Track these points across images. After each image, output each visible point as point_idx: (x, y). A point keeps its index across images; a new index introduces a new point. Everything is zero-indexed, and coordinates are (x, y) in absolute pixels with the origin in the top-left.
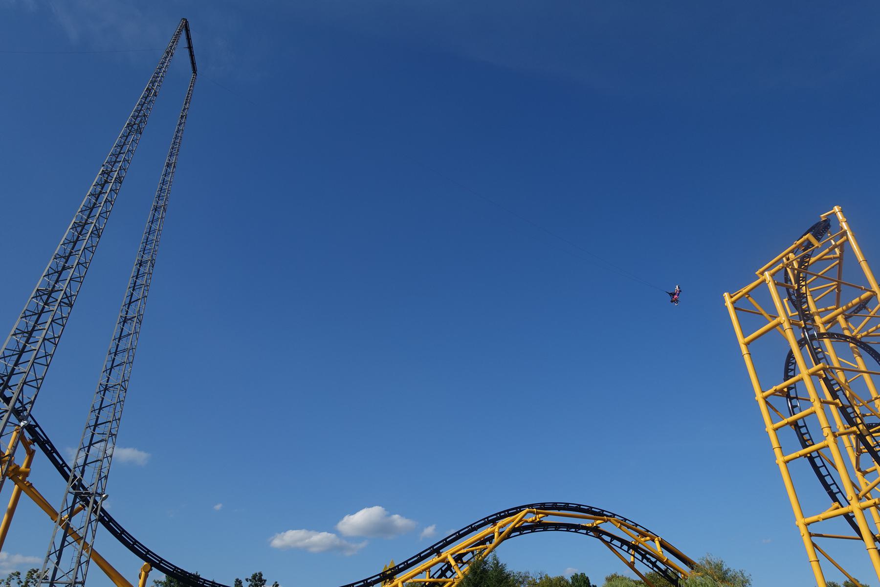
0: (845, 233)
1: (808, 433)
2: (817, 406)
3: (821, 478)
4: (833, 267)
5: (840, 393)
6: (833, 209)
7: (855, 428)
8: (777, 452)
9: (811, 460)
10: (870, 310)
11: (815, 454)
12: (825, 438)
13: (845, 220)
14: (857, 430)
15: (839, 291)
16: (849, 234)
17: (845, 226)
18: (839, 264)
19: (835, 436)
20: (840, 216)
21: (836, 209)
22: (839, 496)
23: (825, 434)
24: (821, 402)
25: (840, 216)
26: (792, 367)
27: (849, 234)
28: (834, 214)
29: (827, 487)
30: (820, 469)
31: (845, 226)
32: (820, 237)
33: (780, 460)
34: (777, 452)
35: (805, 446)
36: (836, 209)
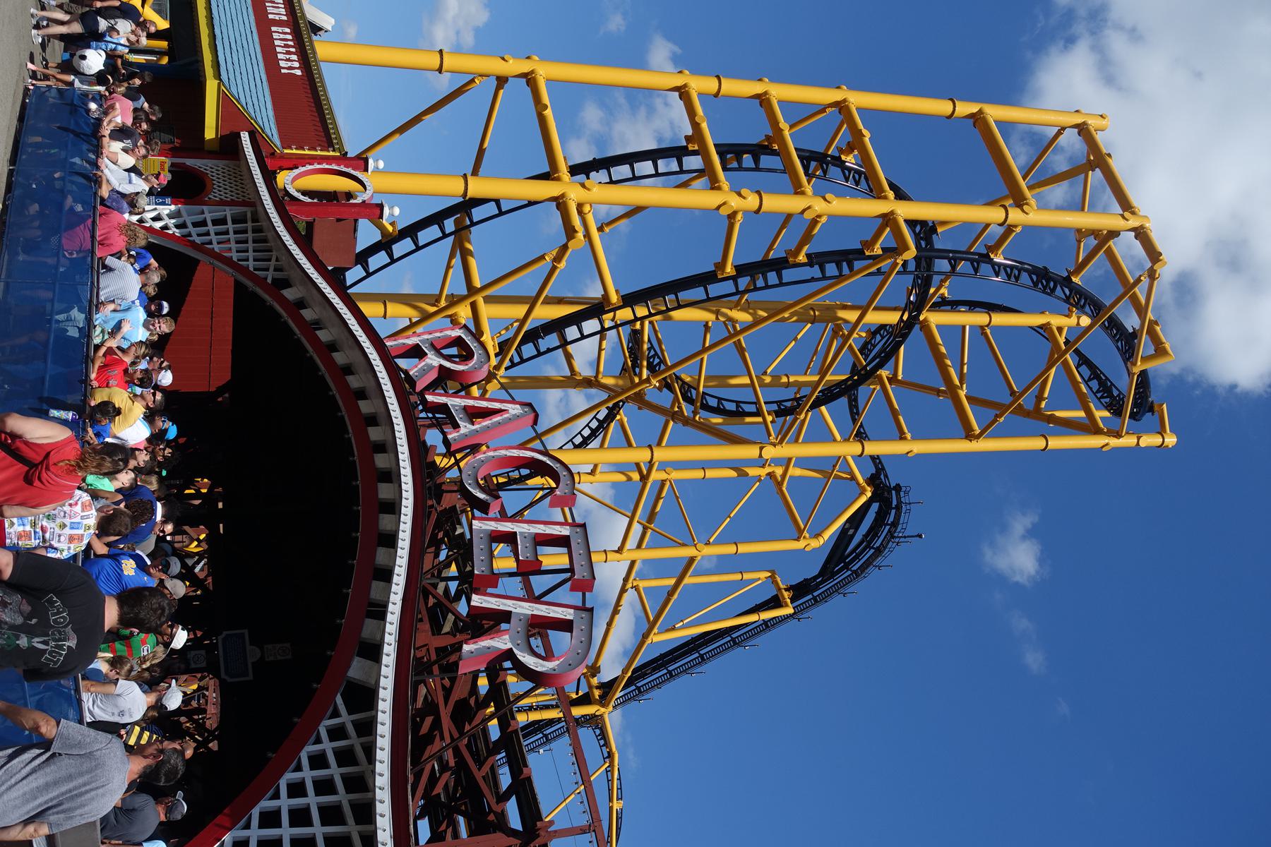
1: (740, 169)
5: (815, 272)
6: (1170, 431)
7: (729, 270)
8: (710, 85)
11: (693, 162)
14: (725, 275)
17: (1128, 441)
20: (1150, 440)
21: (1171, 440)
22: (602, 175)
25: (1150, 440)
28: (1161, 432)
31: (1128, 441)
34: (710, 85)
36: (1171, 440)
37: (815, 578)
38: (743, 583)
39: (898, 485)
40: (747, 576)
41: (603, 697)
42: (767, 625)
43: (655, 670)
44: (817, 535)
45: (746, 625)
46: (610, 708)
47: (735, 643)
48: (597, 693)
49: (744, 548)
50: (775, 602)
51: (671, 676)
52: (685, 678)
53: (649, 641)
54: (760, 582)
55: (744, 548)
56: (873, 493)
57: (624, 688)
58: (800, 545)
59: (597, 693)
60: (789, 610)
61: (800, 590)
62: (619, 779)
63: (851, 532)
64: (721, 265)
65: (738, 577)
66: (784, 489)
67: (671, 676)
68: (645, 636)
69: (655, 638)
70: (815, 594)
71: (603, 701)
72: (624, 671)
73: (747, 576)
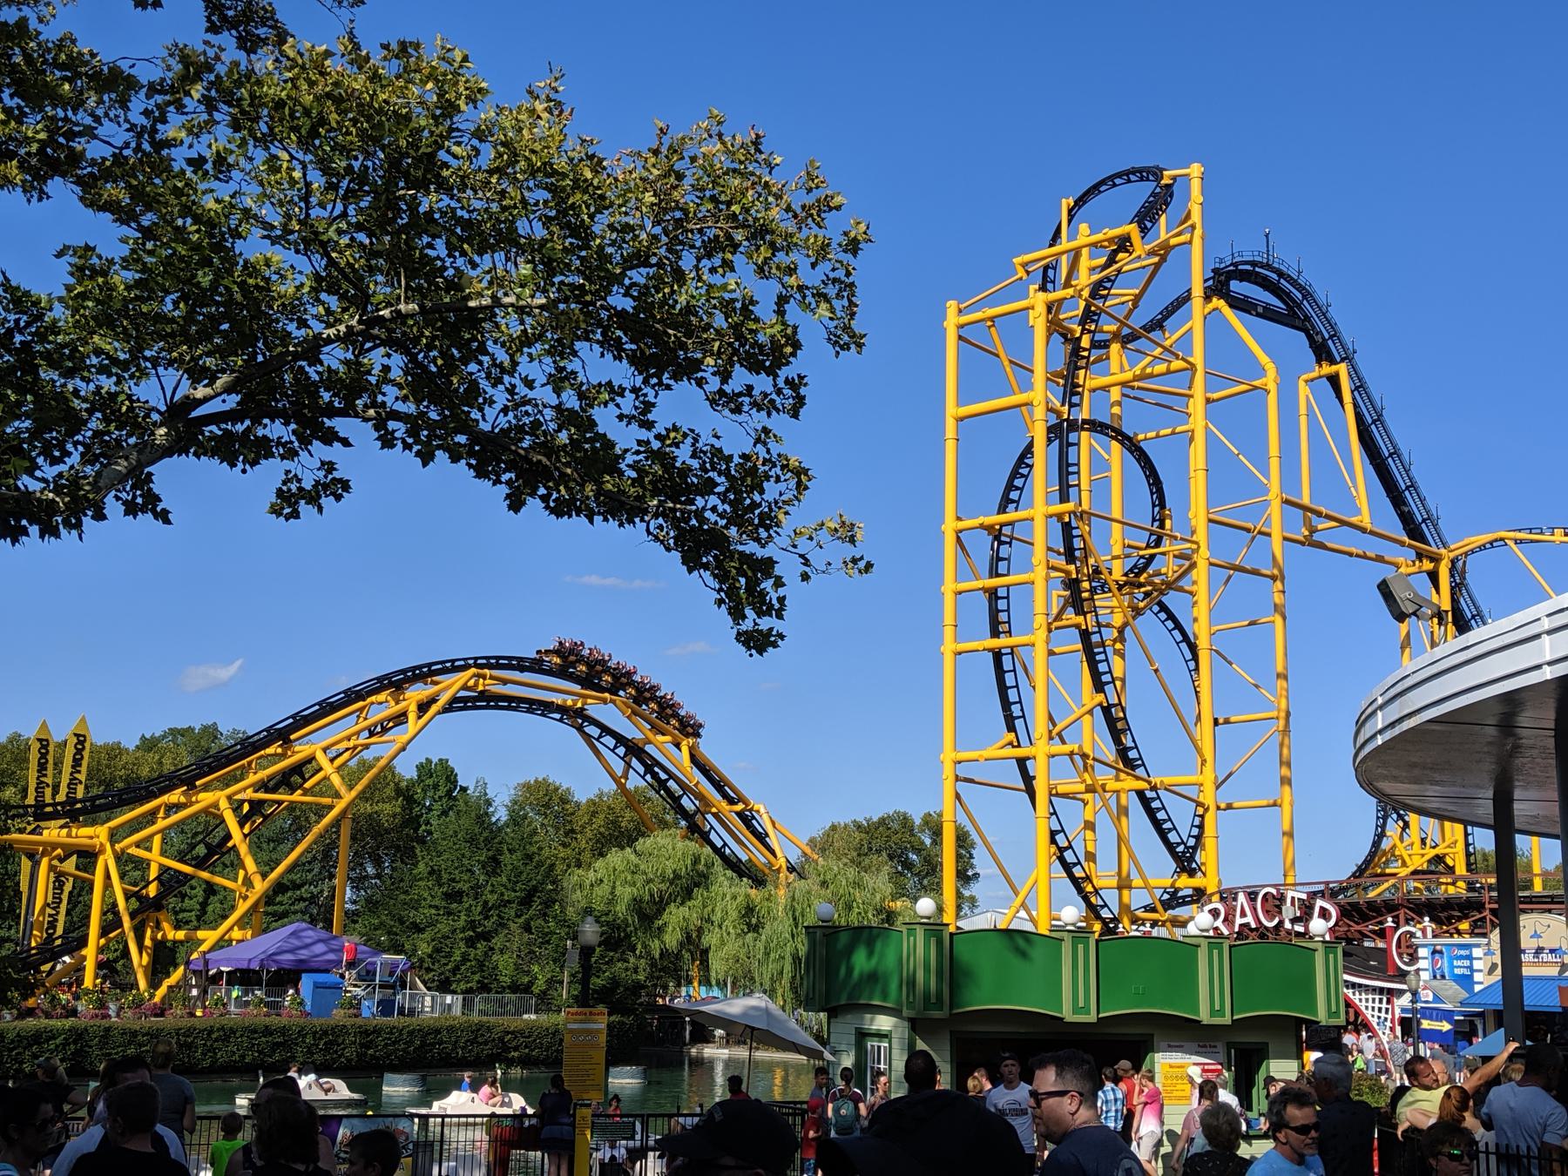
0: (1193, 227)
2: (1040, 573)
3: (1003, 689)
4: (1144, 267)
7: (1080, 619)
9: (997, 656)
10: (1167, 335)
12: (1031, 631)
13: (1201, 200)
15: (1135, 306)
16: (1198, 232)
18: (1157, 266)
19: (1050, 631)
20: (1196, 185)
21: (1195, 170)
23: (1036, 626)
24: (1048, 568)
25: (1196, 185)
26: (1024, 471)
27: (1198, 232)
29: (1006, 704)
30: (1007, 675)
32: (1149, 225)
33: (949, 647)
35: (995, 633)
36: (1195, 170)
37: (1309, 337)
38: (1310, 414)
39: (1213, 271)
40: (1303, 410)
41: (1432, 559)
42: (1359, 387)
43: (1405, 503)
44: (1263, 372)
45: (1356, 406)
46: (1443, 551)
47: (1379, 419)
48: (1428, 565)
49: (1274, 450)
50: (1334, 380)
51: (1412, 486)
52: (1414, 471)
53: (1369, 527)
54: (1311, 396)
55: (1274, 450)
56: (1221, 297)
57: (1424, 540)
58: (1272, 387)
59: (1428, 565)
60: (1342, 369)
61: (1322, 353)
62: (1531, 530)
63: (1260, 310)
64: (1077, 626)
65: (1303, 420)
66: (1215, 396)
67: (1412, 486)
68: (1363, 530)
69: (1365, 519)
70: (1327, 336)
71: (1436, 559)
72: (1402, 544)
73: (1303, 410)
